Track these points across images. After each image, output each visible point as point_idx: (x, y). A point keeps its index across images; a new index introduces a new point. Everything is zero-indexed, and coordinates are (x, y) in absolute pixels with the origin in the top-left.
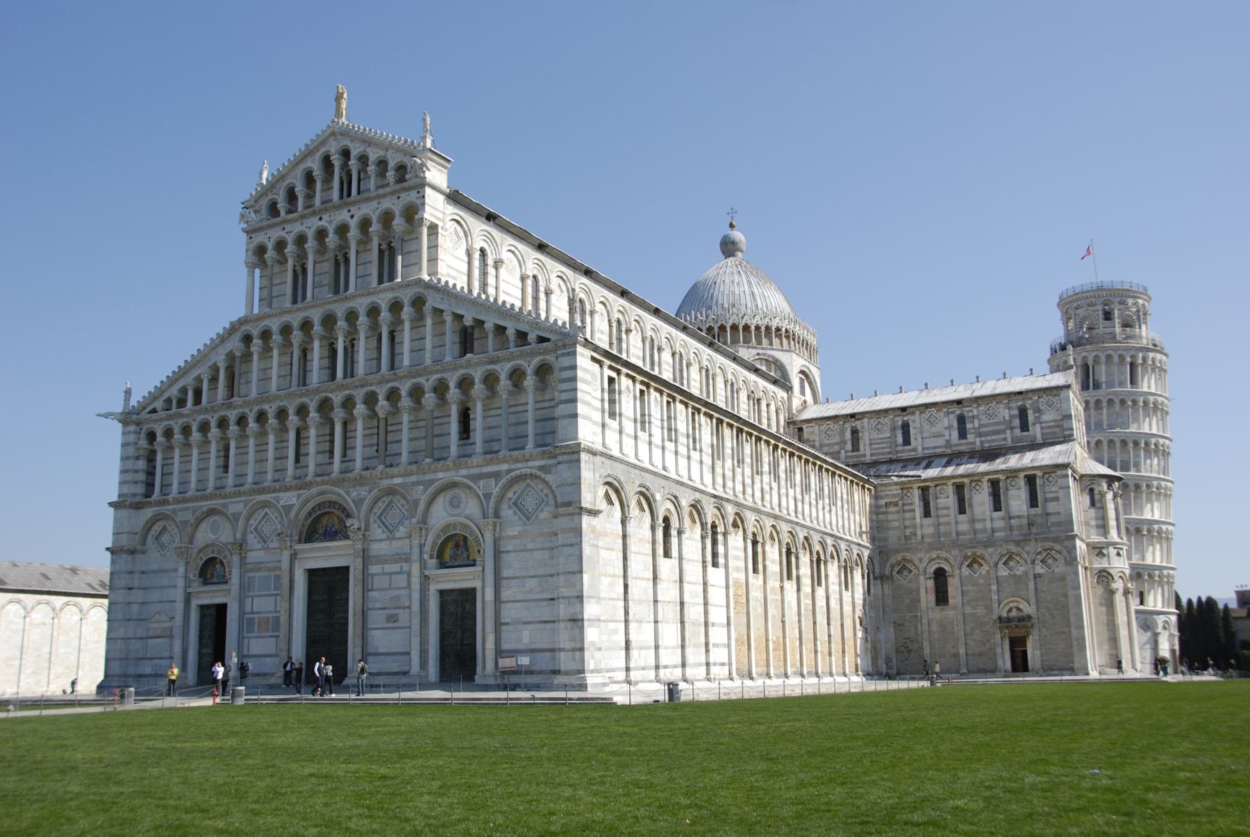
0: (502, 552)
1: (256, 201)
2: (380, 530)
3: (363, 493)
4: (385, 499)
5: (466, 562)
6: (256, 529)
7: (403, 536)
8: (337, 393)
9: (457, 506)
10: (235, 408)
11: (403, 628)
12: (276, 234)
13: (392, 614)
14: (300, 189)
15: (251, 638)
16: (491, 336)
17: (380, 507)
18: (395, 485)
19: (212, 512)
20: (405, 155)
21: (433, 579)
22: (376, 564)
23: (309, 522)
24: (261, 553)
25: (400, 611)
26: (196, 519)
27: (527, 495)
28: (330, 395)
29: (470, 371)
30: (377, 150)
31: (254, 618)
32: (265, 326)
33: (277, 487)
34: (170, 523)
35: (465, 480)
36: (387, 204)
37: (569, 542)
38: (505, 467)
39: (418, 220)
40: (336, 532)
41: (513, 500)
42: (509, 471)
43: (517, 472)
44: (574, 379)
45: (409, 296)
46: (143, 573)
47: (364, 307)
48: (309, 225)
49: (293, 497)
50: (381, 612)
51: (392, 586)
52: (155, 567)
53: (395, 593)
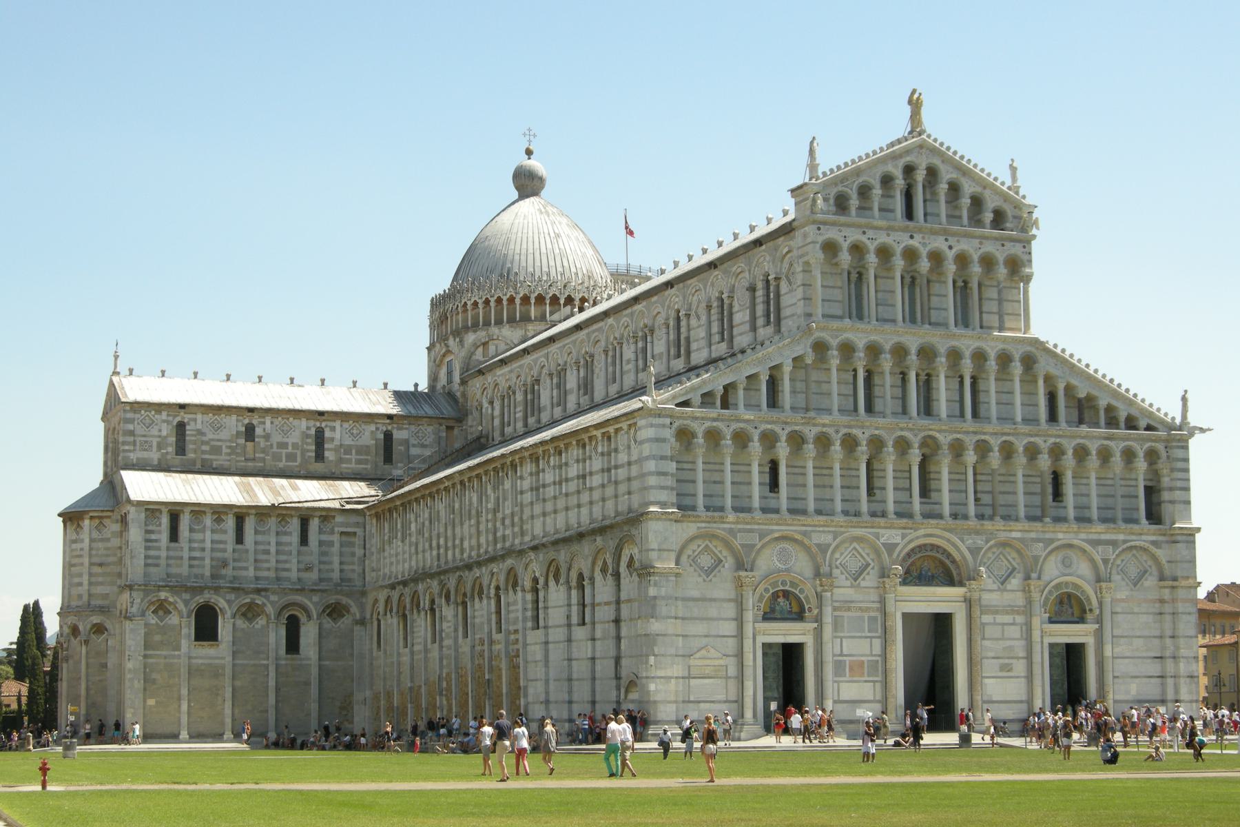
2: (990, 581)
3: (980, 542)
7: (1016, 588)
10: (815, 425)
11: (1018, 677)
12: (854, 236)
13: (1006, 664)
15: (842, 682)
18: (1014, 538)
19: (784, 538)
20: (1005, 201)
24: (851, 591)
28: (937, 435)
31: (845, 661)
32: (847, 339)
36: (989, 247)
37: (1187, 611)
38: (1121, 537)
39: (1027, 276)
41: (1120, 568)
42: (1125, 542)
44: (1187, 470)
47: (970, 350)
49: (897, 535)
51: (1005, 636)
52: (695, 593)
53: (1008, 643)
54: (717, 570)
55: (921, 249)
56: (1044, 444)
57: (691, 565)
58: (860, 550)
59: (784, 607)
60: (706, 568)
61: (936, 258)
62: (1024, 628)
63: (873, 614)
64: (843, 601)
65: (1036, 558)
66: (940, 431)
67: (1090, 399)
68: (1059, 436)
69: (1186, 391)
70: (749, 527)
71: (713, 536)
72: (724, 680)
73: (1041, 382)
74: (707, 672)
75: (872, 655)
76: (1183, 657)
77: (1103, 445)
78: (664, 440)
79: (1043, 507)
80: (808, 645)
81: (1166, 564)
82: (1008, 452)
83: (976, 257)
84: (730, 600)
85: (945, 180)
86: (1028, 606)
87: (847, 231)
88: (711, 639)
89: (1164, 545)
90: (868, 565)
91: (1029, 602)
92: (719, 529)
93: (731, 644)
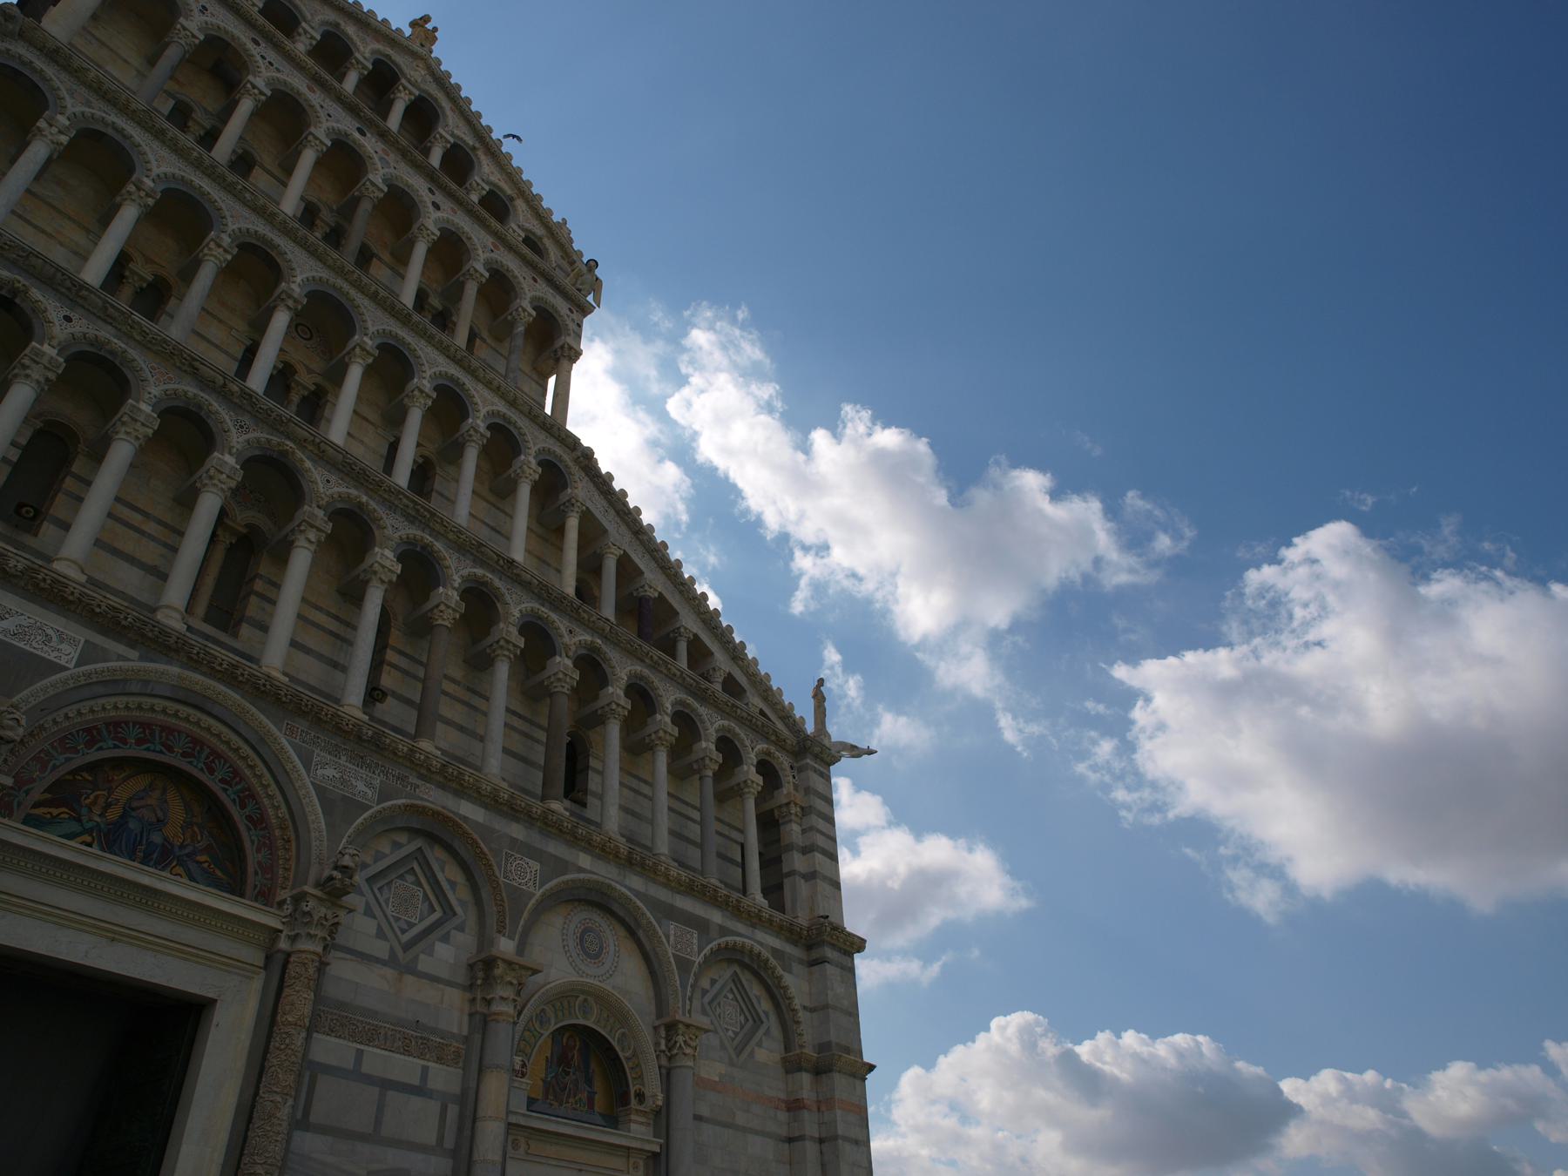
2: (369, 926)
3: (361, 786)
4: (402, 838)
8: (333, 478)
9: (595, 956)
17: (385, 856)
18: (465, 819)
22: (331, 1031)
23: (78, 761)
27: (726, 997)
28: (308, 464)
30: (499, 176)
32: (120, 131)
35: (639, 903)
42: (724, 931)
45: (539, 446)
62: (453, 1111)
86: (478, 1037)
89: (796, 967)
91: (482, 1022)
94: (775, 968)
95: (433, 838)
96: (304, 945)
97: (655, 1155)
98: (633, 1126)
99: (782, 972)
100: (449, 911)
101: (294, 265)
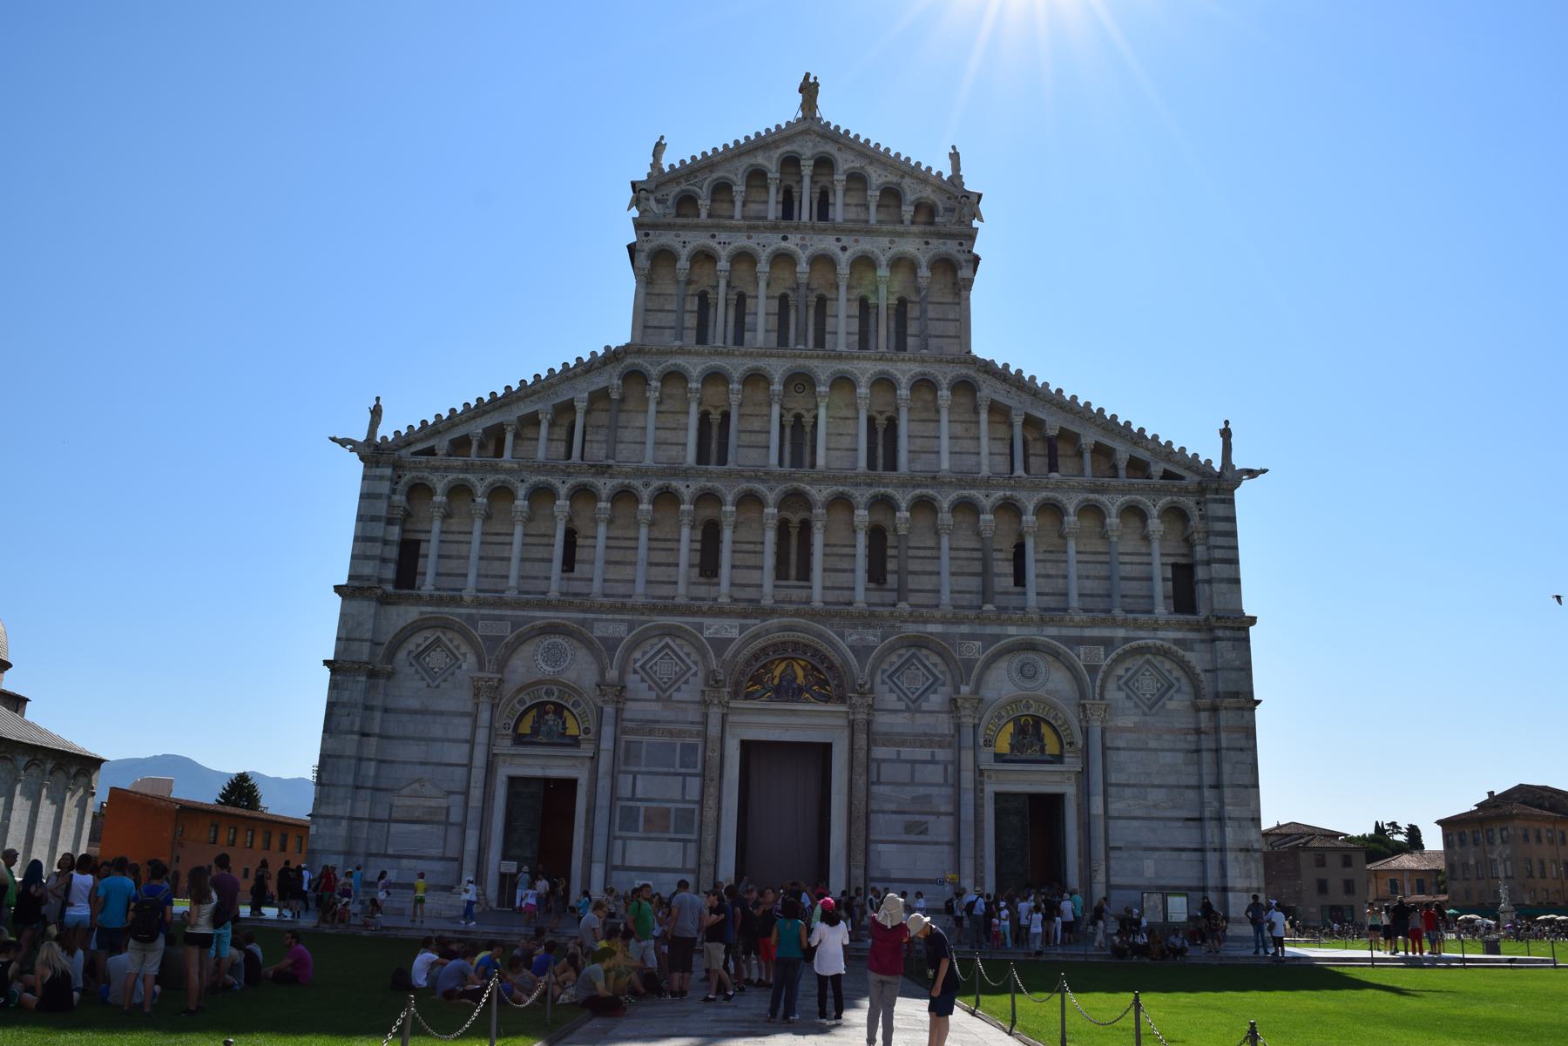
0: (1109, 748)
1: (657, 186)
2: (894, 697)
3: (871, 638)
5: (1038, 756)
6: (642, 667)
7: (935, 709)
8: (822, 487)
9: (1033, 677)
10: (612, 476)
11: (936, 843)
12: (698, 240)
14: (739, 188)
16: (1087, 456)
17: (895, 663)
18: (931, 634)
21: (990, 777)
22: (884, 745)
24: (657, 706)
25: (931, 819)
26: (518, 636)
27: (1143, 674)
28: (808, 488)
29: (1059, 496)
30: (885, 173)
32: (676, 364)
33: (705, 608)
34: (450, 635)
37: (1238, 746)
40: (800, 690)
42: (1126, 640)
43: (1140, 642)
44: (1234, 534)
45: (949, 377)
46: (386, 711)
47: (869, 375)
48: (763, 242)
49: (735, 627)
50: (894, 816)
52: (414, 703)
53: (922, 791)
54: (451, 671)
55: (800, 252)
56: (987, 499)
57: (411, 665)
58: (676, 649)
59: (555, 728)
60: (436, 670)
61: (824, 261)
62: (950, 768)
63: (688, 740)
64: (641, 720)
65: (969, 664)
66: (813, 482)
67: (1067, 436)
68: (1013, 488)
69: (1227, 422)
70: (497, 612)
71: (446, 625)
72: (442, 827)
73: (984, 416)
74: (417, 814)
75: (684, 801)
76: (1230, 818)
77: (1088, 500)
78: (379, 496)
79: (986, 593)
80: (579, 782)
81: (1202, 675)
82: (924, 505)
83: (883, 260)
84: (463, 714)
85: (841, 170)
87: (687, 236)
88: (430, 768)
89: (1197, 646)
90: (689, 669)
91: (958, 727)
92: (452, 614)
93: (460, 773)
94: (1177, 652)
95: (920, 647)
96: (858, 716)
97: (1079, 772)
98: (1066, 760)
99: (1183, 653)
100: (936, 679)
101: (772, 372)
